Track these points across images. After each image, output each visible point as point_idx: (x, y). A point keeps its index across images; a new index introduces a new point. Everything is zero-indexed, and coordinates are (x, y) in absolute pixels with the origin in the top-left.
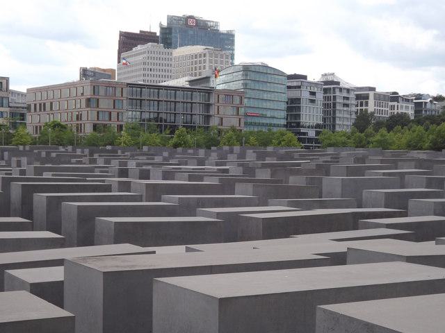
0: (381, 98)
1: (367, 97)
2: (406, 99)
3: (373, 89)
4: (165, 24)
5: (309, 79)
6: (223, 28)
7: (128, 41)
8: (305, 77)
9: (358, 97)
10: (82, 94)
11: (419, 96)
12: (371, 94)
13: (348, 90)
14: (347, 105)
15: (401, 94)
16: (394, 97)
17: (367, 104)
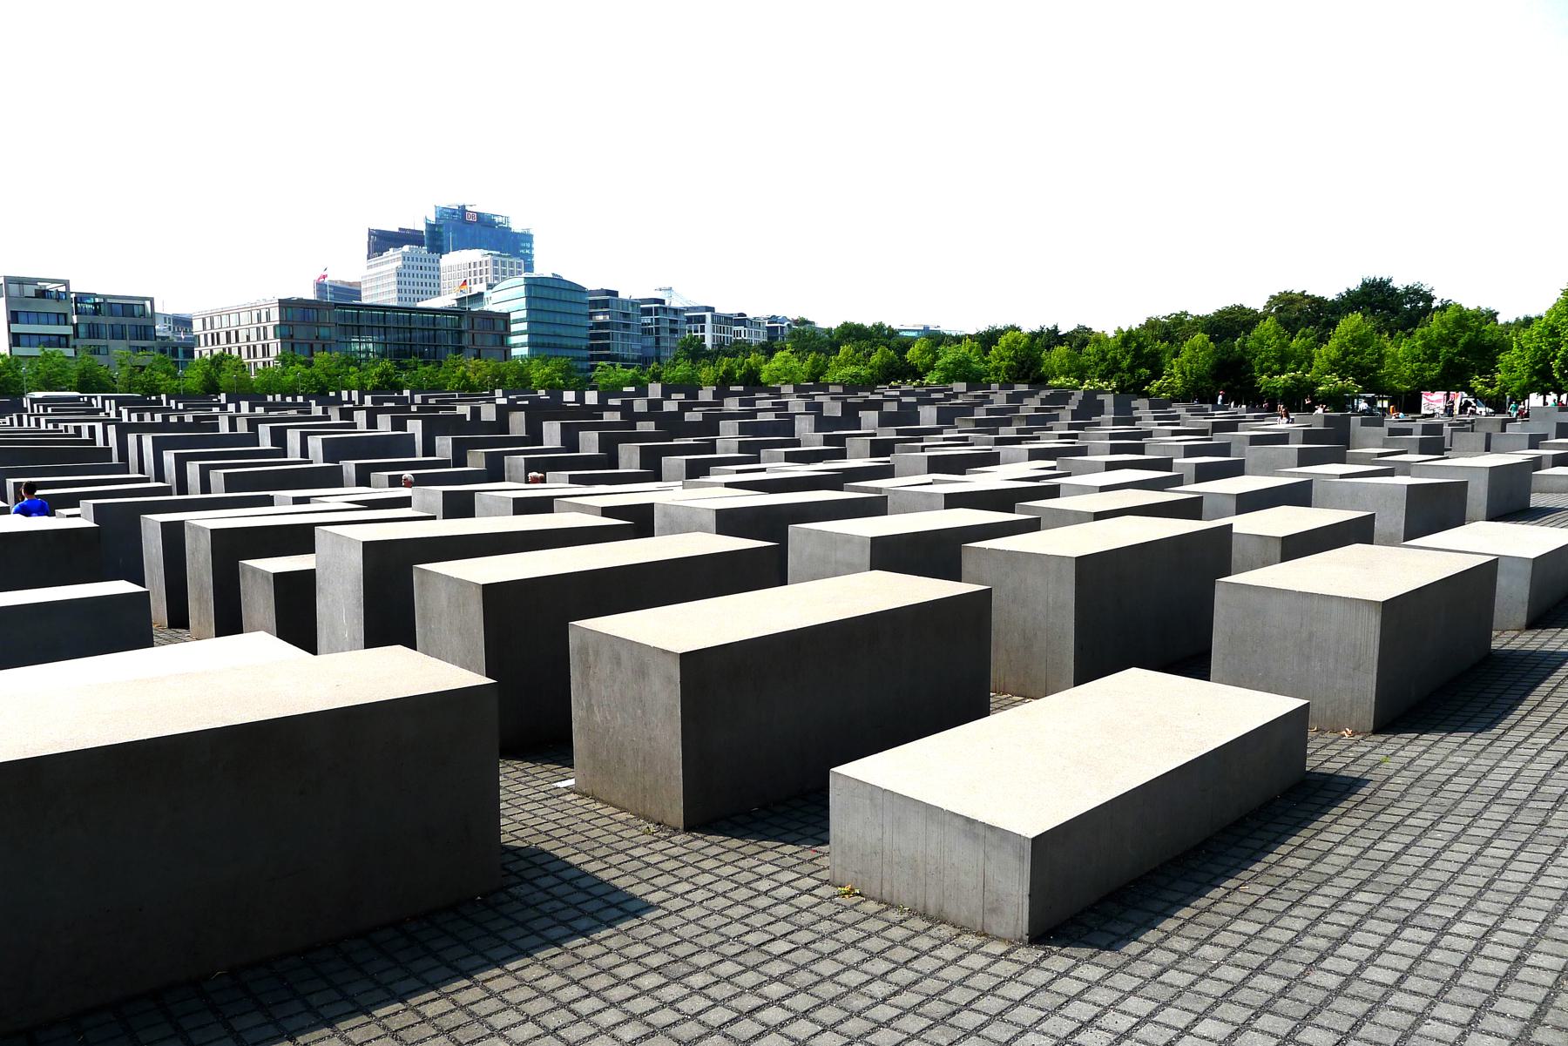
0: (724, 321)
1: (702, 319)
2: (755, 323)
3: (711, 309)
4: (433, 220)
5: (621, 296)
6: (517, 227)
7: (381, 242)
8: (615, 293)
9: (690, 320)
10: (268, 320)
11: (773, 319)
12: (708, 315)
13: (676, 311)
14: (673, 331)
15: (750, 316)
16: (741, 320)
17: (703, 330)
